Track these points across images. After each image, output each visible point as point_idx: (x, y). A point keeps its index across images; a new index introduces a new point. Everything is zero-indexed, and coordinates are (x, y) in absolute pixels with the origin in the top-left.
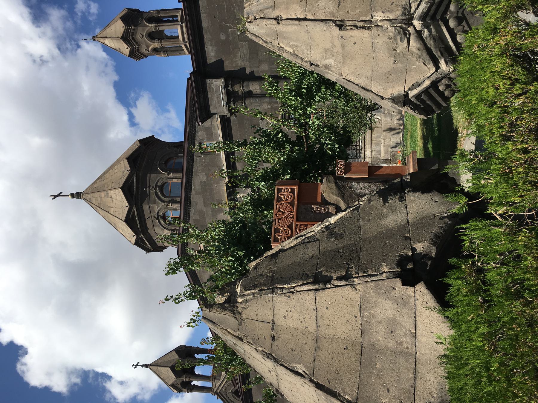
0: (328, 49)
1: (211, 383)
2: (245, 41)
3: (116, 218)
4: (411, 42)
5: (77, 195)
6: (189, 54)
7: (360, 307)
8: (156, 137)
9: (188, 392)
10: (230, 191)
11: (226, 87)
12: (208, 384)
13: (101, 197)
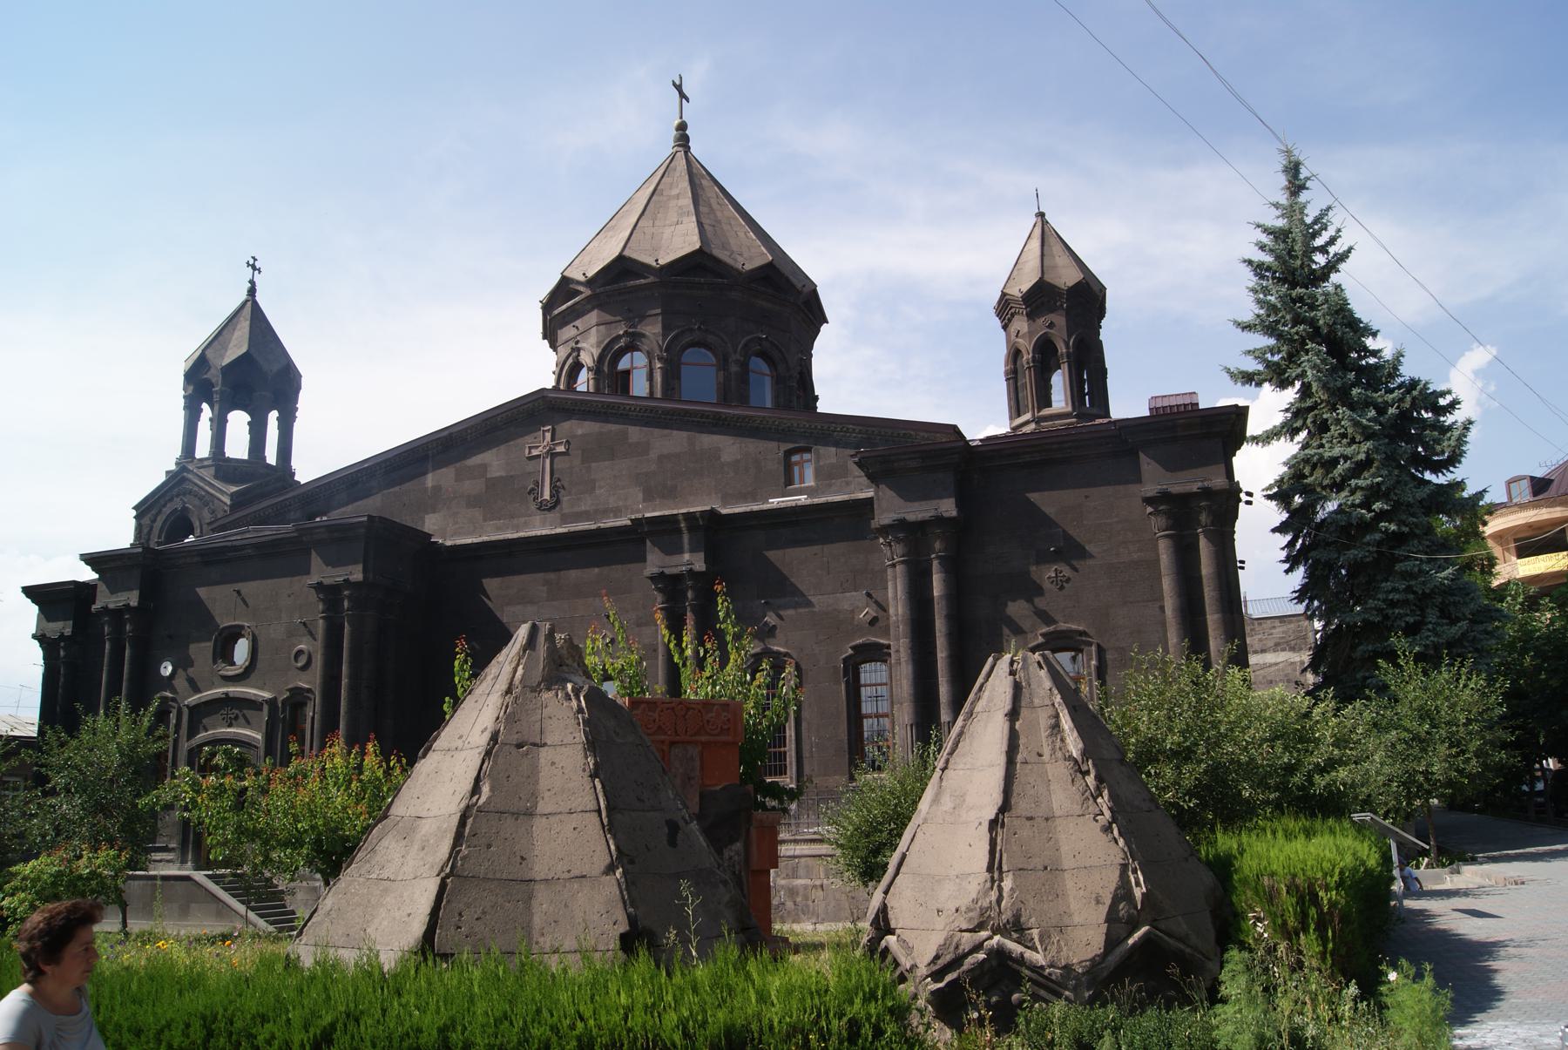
0: (964, 800)
1: (207, 456)
3: (627, 234)
4: (966, 935)
5: (683, 140)
6: (1012, 429)
7: (584, 877)
8: (824, 328)
9: (184, 397)
10: (697, 519)
11: (939, 520)
12: (203, 449)
13: (678, 197)
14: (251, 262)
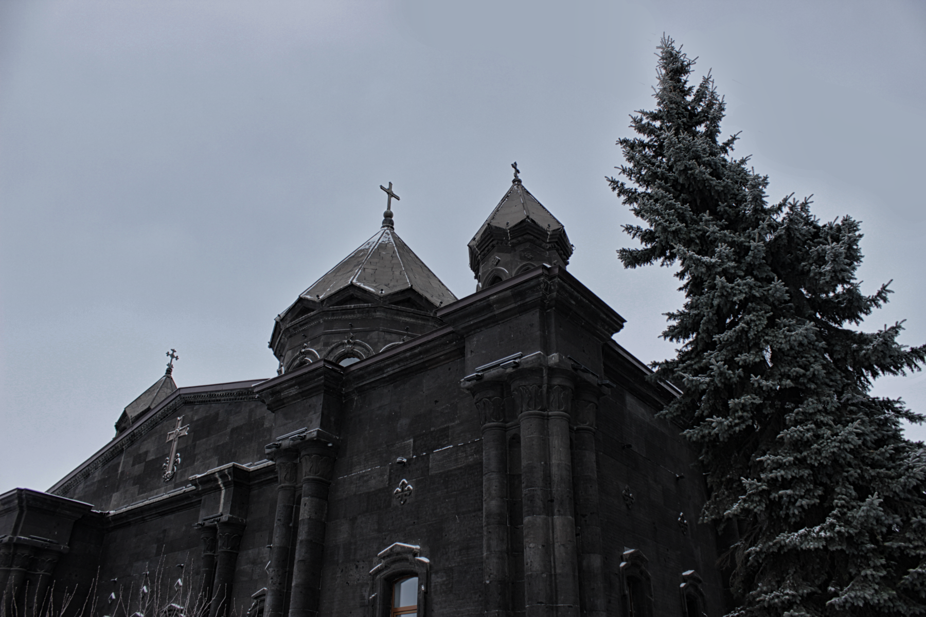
2: (390, 479)
14: (171, 352)
